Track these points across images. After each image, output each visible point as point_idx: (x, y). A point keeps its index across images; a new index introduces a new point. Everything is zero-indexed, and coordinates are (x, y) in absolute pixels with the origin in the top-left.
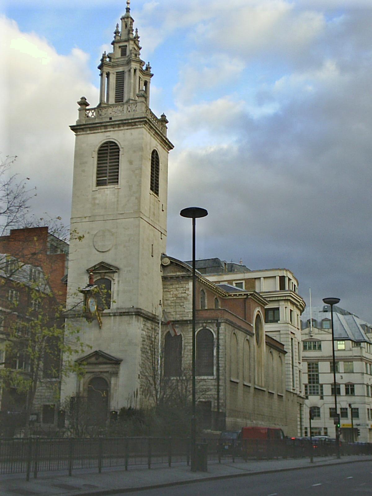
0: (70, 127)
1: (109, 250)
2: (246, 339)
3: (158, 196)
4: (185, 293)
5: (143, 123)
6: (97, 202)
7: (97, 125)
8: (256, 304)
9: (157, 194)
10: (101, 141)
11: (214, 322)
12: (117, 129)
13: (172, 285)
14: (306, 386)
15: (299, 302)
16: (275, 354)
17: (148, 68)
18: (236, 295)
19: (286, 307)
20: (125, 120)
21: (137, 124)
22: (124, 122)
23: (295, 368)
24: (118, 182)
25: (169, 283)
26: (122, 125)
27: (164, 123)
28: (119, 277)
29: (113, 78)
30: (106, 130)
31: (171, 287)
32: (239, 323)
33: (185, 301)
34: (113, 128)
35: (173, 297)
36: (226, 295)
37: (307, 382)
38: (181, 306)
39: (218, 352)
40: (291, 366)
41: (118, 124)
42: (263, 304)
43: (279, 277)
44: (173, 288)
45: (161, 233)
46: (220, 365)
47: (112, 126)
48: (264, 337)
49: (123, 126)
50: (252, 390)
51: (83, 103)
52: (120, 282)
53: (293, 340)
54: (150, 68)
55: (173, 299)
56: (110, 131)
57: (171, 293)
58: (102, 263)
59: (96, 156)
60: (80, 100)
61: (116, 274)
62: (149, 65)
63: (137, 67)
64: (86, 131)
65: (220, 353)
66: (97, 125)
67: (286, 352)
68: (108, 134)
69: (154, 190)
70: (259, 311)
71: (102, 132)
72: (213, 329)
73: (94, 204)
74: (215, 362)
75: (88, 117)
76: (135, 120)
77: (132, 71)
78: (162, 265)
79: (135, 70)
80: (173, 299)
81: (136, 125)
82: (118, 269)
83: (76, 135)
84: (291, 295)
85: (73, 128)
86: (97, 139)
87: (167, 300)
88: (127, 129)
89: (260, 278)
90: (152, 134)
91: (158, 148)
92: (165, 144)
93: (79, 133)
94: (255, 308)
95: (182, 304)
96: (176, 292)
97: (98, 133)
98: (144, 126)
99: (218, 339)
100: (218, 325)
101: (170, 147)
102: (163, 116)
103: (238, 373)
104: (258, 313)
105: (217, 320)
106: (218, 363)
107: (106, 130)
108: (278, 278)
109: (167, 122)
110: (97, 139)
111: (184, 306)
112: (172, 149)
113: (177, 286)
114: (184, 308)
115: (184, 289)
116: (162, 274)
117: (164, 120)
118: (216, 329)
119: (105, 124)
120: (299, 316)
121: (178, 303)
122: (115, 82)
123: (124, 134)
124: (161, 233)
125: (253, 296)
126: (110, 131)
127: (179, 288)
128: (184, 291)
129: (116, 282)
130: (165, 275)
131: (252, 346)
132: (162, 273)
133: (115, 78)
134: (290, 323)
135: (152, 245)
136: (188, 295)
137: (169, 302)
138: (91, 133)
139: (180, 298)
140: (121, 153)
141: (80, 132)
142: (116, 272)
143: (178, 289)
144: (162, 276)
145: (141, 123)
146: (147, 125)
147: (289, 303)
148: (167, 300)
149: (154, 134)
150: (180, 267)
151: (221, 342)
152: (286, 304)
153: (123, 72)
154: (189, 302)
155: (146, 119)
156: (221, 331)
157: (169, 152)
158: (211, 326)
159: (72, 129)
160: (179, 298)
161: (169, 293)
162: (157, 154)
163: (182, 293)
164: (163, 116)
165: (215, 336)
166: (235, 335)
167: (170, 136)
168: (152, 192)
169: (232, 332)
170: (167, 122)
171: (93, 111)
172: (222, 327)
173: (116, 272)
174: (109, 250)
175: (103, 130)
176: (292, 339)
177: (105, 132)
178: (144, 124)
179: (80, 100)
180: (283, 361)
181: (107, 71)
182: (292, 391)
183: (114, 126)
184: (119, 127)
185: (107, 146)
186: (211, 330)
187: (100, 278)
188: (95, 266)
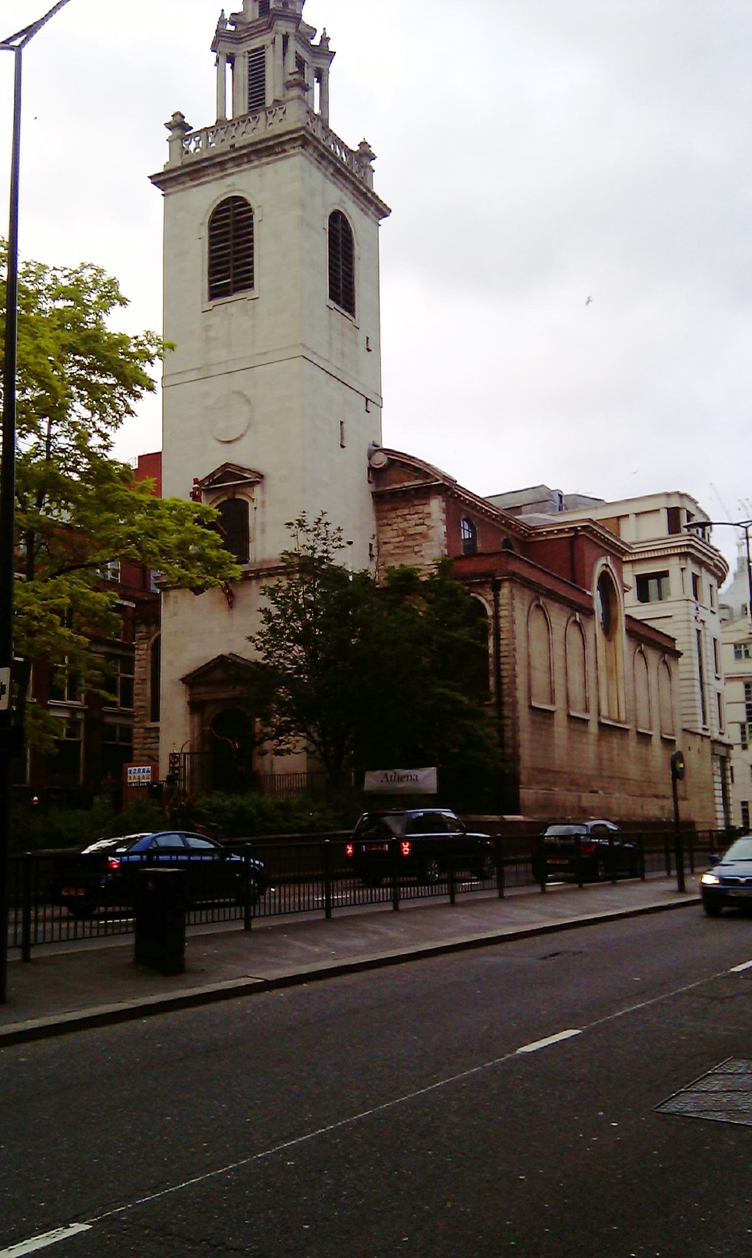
0: (150, 177)
1: (242, 436)
2: (571, 620)
4: (423, 524)
5: (299, 143)
6: (212, 334)
8: (600, 551)
9: (352, 311)
11: (487, 582)
12: (245, 166)
13: (395, 509)
14: (743, 726)
15: (712, 559)
16: (653, 657)
17: (325, 39)
18: (552, 531)
19: (682, 569)
20: (260, 142)
21: (287, 147)
22: (260, 146)
23: (706, 687)
24: (251, 286)
25: (387, 507)
26: (253, 158)
27: (365, 160)
28: (263, 492)
29: (242, 64)
30: (225, 173)
31: (393, 515)
32: (562, 590)
33: (423, 540)
34: (238, 165)
35: (398, 536)
36: (530, 534)
37: (743, 718)
38: (416, 553)
39: (497, 645)
40: (697, 683)
42: (619, 551)
43: (666, 511)
44: (397, 517)
45: (367, 399)
46: (504, 674)
47: (236, 162)
48: (622, 623)
49: (259, 158)
50: (593, 728)
51: (179, 125)
52: (267, 504)
53: (702, 633)
54: (329, 39)
55: (398, 539)
56: (233, 174)
57: (395, 527)
58: (227, 465)
59: (205, 233)
61: (257, 489)
62: (325, 33)
63: (289, 30)
64: (183, 183)
65: (502, 648)
67: (679, 654)
68: (229, 181)
69: (342, 302)
70: (607, 566)
71: (216, 179)
72: (485, 599)
73: (208, 340)
74: (491, 667)
75: (187, 152)
77: (279, 40)
78: (371, 469)
79: (286, 38)
80: (398, 539)
81: (284, 151)
82: (262, 476)
84: (692, 543)
86: (207, 196)
87: (386, 543)
88: (268, 163)
89: (627, 516)
91: (346, 206)
92: (366, 203)
93: (169, 191)
94: (596, 560)
95: (417, 549)
96: (405, 525)
98: (301, 149)
99: (497, 617)
100: (496, 588)
101: (383, 211)
102: (364, 144)
103: (552, 692)
104: (604, 568)
105: (493, 577)
106: (498, 670)
107: (225, 173)
108: (664, 514)
110: (207, 196)
111: (422, 553)
112: (386, 216)
113: (406, 511)
114: (422, 556)
115: (421, 516)
116: (371, 488)
117: (365, 154)
118: (490, 597)
119: (218, 160)
120: (715, 588)
121: (410, 547)
122: (246, 73)
123: (260, 175)
124: (367, 399)
125: (589, 532)
126: (233, 174)
127: (409, 514)
128: (421, 521)
129: (259, 506)
130: (380, 489)
131: (590, 637)
132: (373, 484)
133: (247, 64)
134: (693, 599)
135: (342, 423)
136: (430, 527)
137: (389, 547)
138: (194, 186)
139: (413, 537)
140: (256, 219)
141: (171, 187)
142: (258, 482)
143: (408, 516)
144: (372, 493)
145: (295, 145)
147: (689, 561)
148: (386, 543)
150: (412, 469)
151: (503, 623)
152: (683, 561)
153: (263, 47)
154: (433, 543)
155: (303, 132)
156: (503, 601)
157: (380, 222)
158: (480, 591)
159: (154, 183)
160: (411, 538)
161: (390, 528)
162: (345, 222)
163: (416, 525)
164: (364, 144)
165: (490, 612)
166: (541, 613)
167: (382, 186)
168: (333, 304)
169: (569, 620)
171: (197, 139)
172: (505, 591)
173: (258, 482)
174: (242, 436)
175: (218, 175)
176: (698, 631)
177: (222, 178)
179: (170, 119)
180: (673, 670)
181: (228, 51)
182: (700, 731)
183: (239, 161)
184: (249, 161)
185: (227, 210)
186: (480, 598)
187: (225, 498)
188: (213, 474)
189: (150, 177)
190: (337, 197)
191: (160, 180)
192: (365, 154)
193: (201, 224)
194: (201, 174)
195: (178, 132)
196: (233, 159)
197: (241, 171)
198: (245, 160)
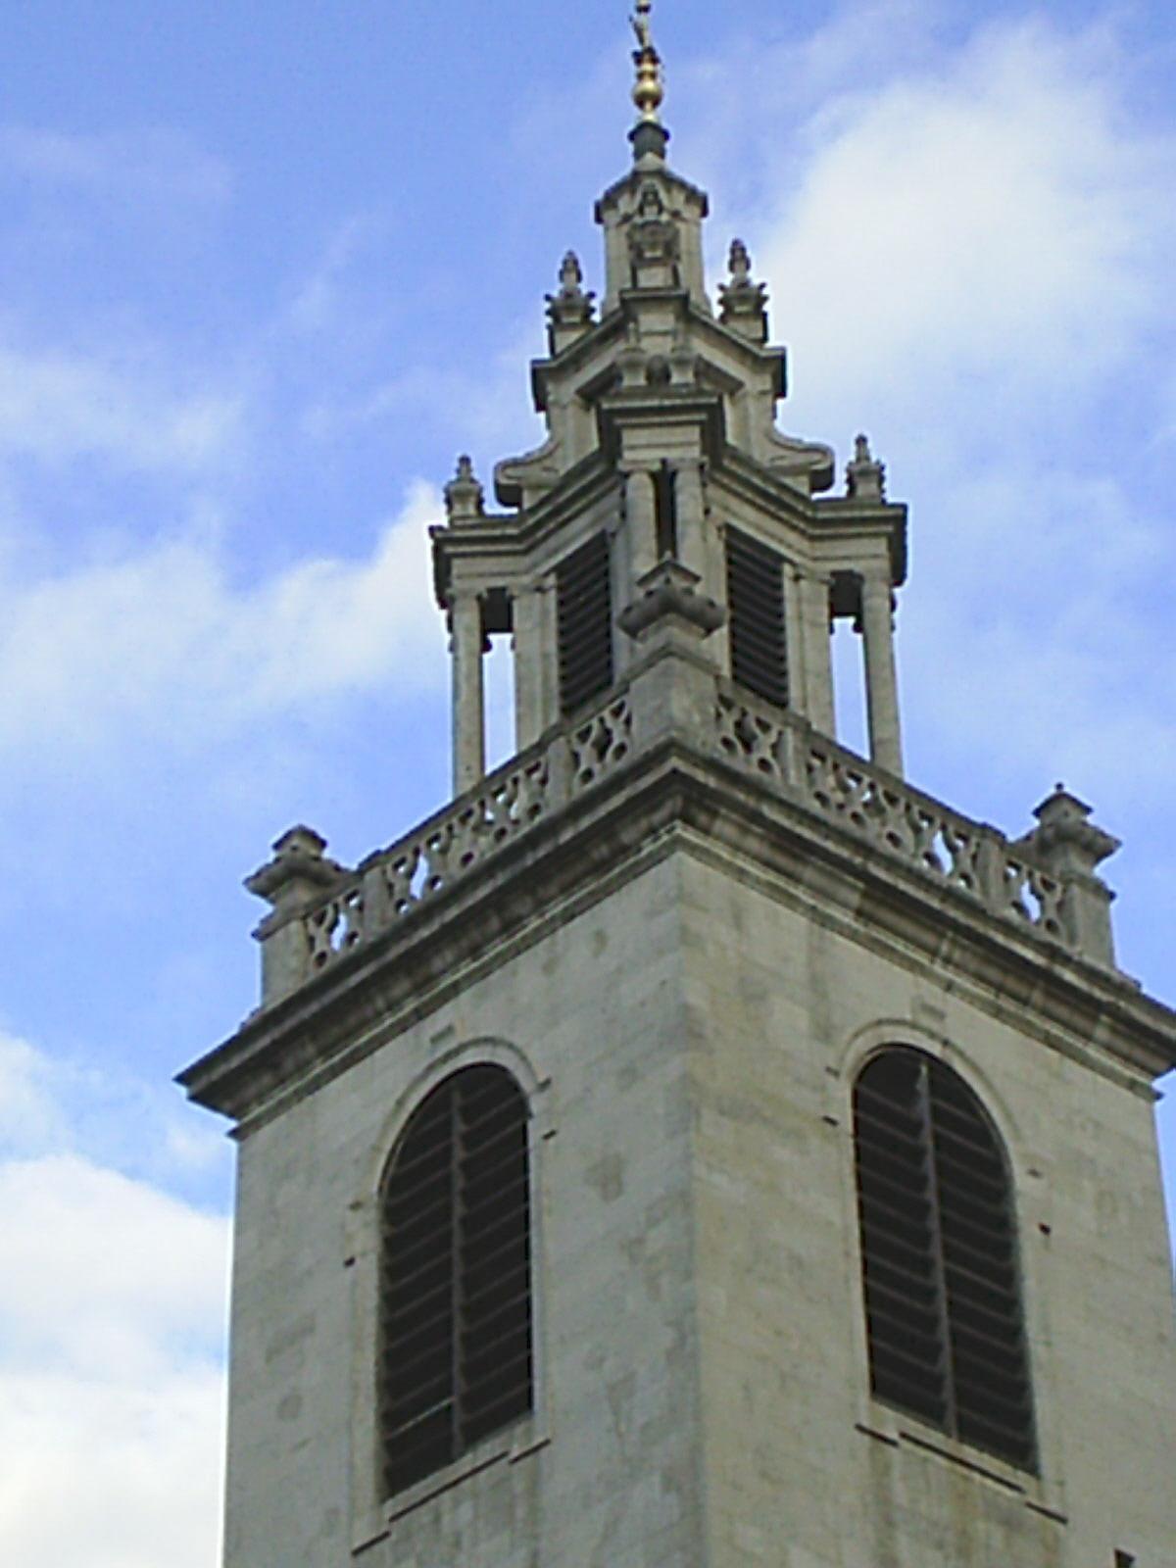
0: (181, 1079)
3: (1033, 1470)
5: (673, 804)
7: (354, 980)
10: (400, 1103)
34: (475, 952)
41: (497, 901)
47: (465, 943)
60: (272, 856)
64: (302, 1067)
66: (354, 980)
76: (602, 811)
81: (625, 850)
83: (234, 1134)
85: (203, 1082)
88: (569, 916)
90: (846, 918)
97: (380, 1041)
98: (681, 830)
109: (1099, 847)
123: (548, 968)
146: (719, 826)
149: (859, 913)
159: (194, 1098)
170: (1099, 847)
178: (689, 821)
183: (475, 935)
184: (509, 926)
189: (181, 1079)
190: (888, 994)
191: (216, 1083)
192: (1066, 836)
193: (356, 1206)
194: (352, 1020)
195: (302, 895)
196: (449, 933)
197: (484, 972)
198: (495, 924)
